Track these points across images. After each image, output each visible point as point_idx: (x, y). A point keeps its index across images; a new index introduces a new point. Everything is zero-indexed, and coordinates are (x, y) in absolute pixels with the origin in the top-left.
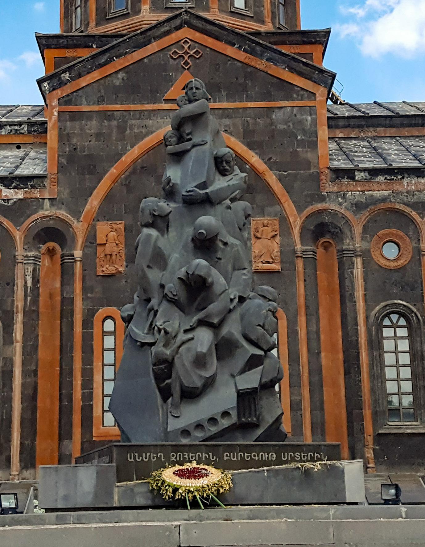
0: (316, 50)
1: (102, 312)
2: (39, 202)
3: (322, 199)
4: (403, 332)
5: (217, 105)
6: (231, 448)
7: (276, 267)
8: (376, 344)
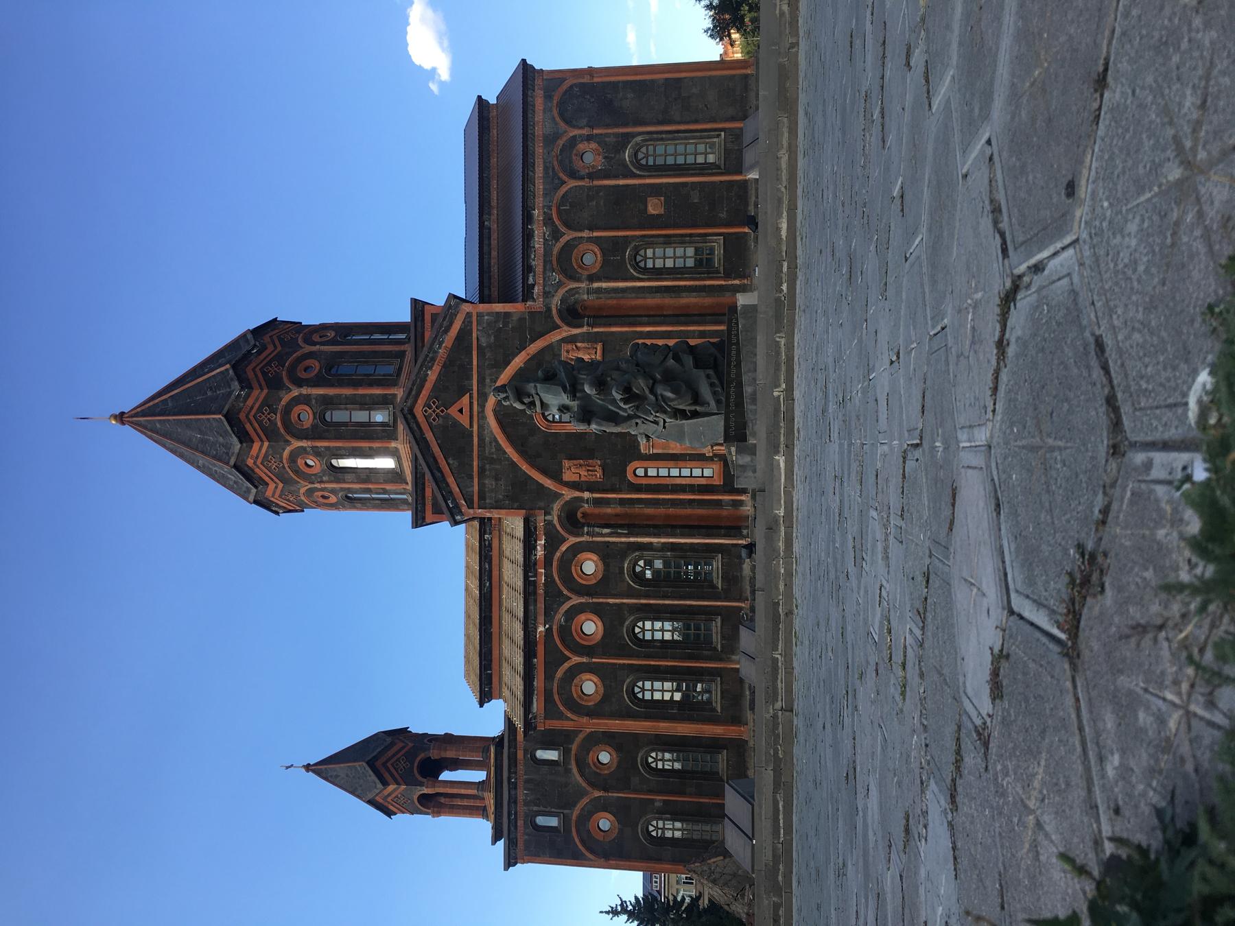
0: (428, 313)
1: (630, 477)
2: (549, 524)
3: (549, 310)
4: (649, 252)
5: (475, 388)
6: (729, 373)
7: (599, 347)
8: (658, 273)
